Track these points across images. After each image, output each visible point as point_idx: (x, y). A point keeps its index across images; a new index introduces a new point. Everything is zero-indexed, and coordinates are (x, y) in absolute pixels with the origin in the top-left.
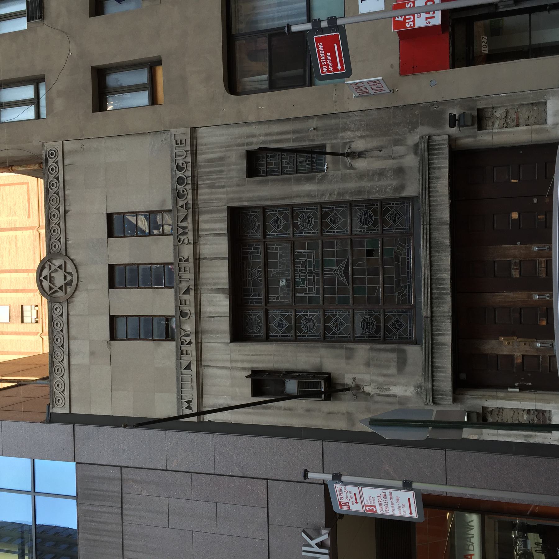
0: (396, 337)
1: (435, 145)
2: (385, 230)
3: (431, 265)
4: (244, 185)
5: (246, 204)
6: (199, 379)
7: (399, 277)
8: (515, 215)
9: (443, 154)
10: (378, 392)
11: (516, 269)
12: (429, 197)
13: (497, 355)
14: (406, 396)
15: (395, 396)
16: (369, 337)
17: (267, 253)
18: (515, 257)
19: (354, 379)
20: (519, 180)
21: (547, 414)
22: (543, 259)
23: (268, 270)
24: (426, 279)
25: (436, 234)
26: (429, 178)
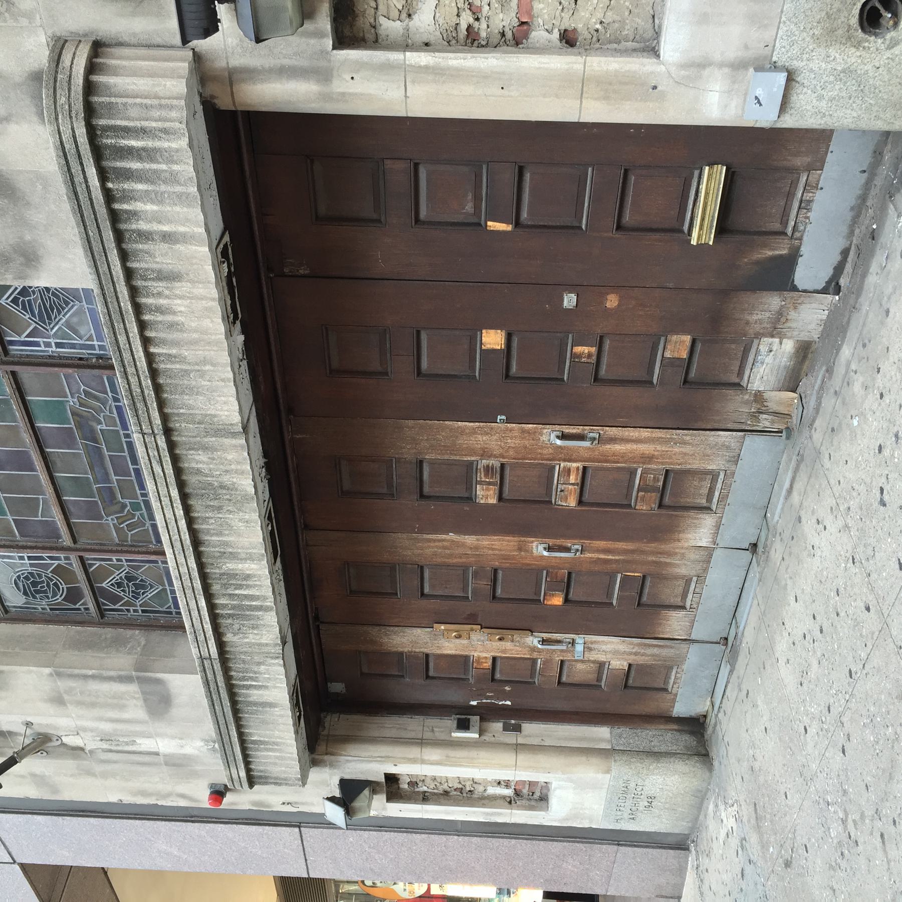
0: (135, 611)
1: (127, 131)
2: (12, 343)
3: (196, 543)
7: (107, 479)
8: (493, 339)
9: (173, 178)
10: (105, 746)
11: (489, 484)
12: (146, 342)
13: (427, 655)
14: (185, 755)
15: (157, 754)
18: (485, 453)
19: (28, 724)
20: (517, 224)
21: (543, 803)
22: (575, 465)
24: (186, 578)
25: (196, 461)
26: (129, 274)
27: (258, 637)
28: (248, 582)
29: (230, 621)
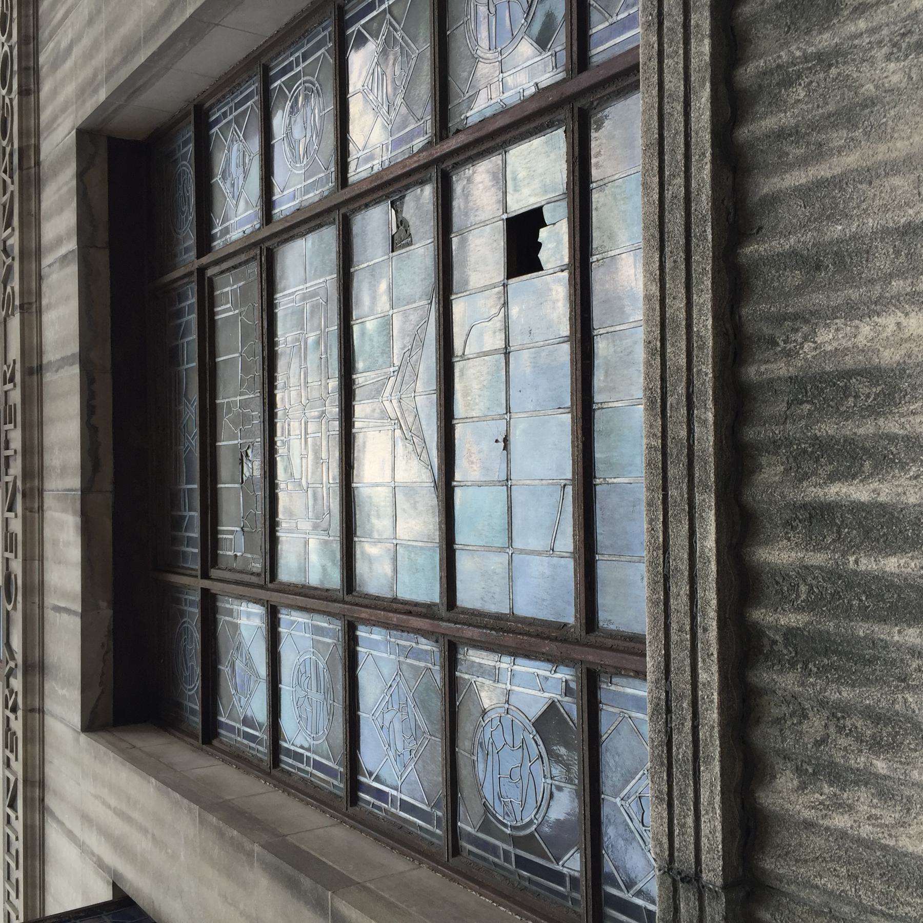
4: (99, 11)
5: (102, 95)
6: (33, 856)
16: (521, 862)
17: (213, 322)
23: (214, 407)
27: (890, 816)
28: (891, 426)
29: (787, 681)
